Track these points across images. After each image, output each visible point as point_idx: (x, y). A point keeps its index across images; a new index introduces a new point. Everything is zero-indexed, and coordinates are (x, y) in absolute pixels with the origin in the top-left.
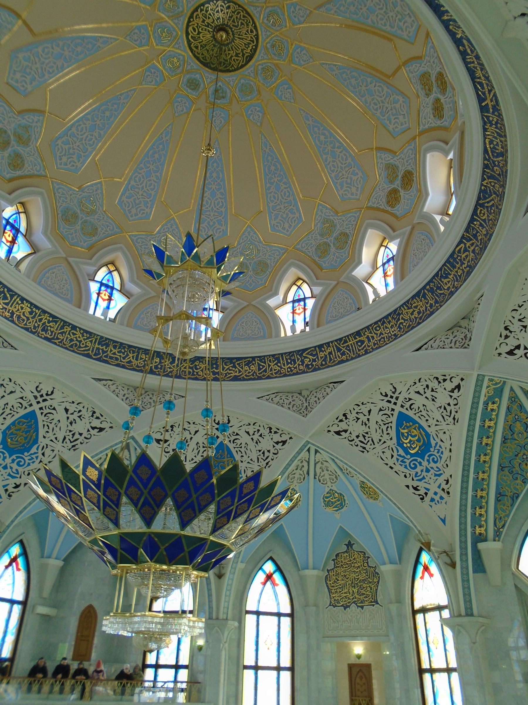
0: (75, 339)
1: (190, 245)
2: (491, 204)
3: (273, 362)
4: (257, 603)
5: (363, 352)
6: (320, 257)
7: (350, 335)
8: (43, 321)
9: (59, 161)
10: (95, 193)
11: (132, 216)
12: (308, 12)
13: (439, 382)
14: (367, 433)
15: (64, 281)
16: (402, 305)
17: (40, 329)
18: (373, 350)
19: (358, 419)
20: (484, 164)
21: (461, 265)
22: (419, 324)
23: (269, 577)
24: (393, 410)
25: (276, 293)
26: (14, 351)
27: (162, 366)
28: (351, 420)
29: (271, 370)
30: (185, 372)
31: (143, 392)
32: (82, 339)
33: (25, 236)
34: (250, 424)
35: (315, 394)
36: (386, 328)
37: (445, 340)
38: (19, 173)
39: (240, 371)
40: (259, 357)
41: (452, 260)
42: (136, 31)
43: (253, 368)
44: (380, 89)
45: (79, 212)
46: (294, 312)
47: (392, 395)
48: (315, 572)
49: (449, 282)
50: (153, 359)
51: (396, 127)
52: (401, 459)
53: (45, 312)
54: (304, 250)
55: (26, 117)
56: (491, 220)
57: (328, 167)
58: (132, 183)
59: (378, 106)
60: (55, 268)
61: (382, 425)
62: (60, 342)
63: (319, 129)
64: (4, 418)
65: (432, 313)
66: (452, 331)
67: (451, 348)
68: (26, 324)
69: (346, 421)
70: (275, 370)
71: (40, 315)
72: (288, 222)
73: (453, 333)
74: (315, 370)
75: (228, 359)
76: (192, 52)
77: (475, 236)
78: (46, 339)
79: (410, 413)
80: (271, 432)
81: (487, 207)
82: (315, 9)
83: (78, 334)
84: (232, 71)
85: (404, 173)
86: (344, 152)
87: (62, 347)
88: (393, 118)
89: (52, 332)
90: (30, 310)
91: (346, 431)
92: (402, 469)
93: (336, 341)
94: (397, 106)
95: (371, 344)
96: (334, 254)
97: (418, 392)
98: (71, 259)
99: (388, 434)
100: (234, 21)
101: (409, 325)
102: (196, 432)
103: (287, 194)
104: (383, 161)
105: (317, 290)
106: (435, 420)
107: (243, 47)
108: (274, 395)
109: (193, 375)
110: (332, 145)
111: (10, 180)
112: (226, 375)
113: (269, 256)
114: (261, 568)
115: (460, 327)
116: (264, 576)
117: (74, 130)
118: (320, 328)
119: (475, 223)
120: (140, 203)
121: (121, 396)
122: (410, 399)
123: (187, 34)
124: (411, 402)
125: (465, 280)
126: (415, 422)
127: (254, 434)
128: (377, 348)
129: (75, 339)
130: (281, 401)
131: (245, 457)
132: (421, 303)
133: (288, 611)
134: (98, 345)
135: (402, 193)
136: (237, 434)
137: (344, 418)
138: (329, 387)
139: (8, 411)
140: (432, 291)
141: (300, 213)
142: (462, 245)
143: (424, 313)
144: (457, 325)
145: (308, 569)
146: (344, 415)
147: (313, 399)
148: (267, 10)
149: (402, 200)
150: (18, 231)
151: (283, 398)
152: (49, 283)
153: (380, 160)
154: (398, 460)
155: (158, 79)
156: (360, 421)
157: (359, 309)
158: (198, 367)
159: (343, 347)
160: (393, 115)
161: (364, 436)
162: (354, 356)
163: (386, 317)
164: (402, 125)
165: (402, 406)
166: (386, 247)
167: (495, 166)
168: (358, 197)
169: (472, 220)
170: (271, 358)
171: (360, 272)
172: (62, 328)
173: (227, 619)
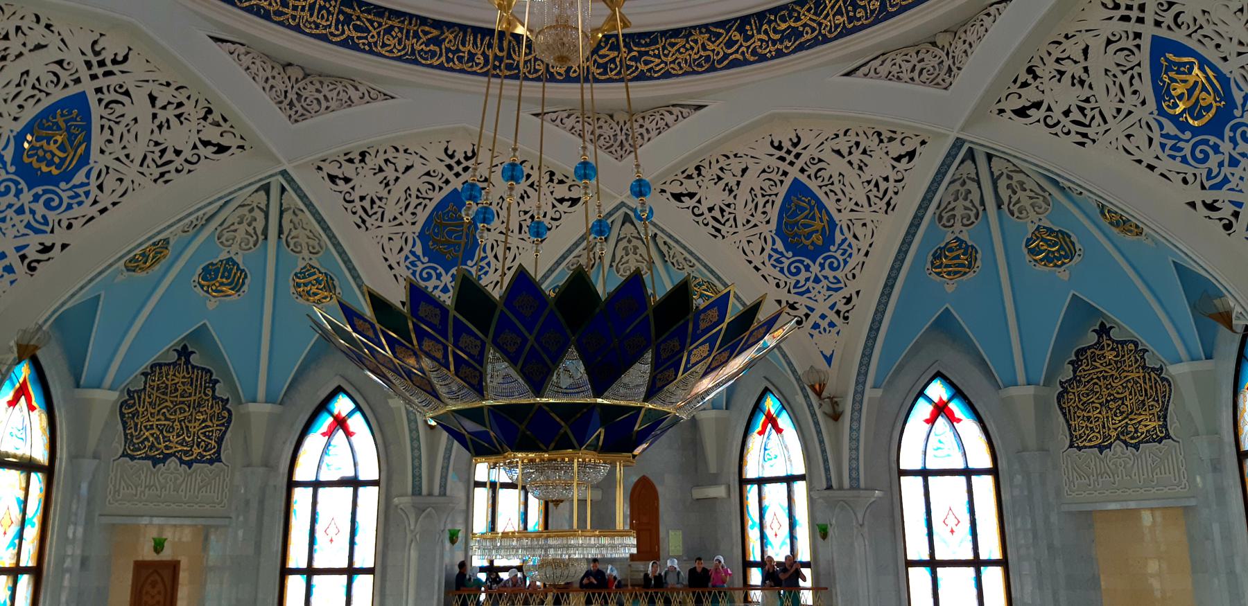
4: (921, 456)
23: (941, 409)
34: (837, 136)
48: (1031, 390)
52: (1170, 143)
64: (413, 214)
80: (881, 141)
92: (1177, 165)
102: (744, 171)
106: (1235, 41)
114: (921, 394)
116: (930, 408)
127: (850, 153)
131: (844, 202)
133: (987, 463)
136: (820, 160)
139: (414, 202)
145: (1016, 385)
154: (1163, 146)
173: (858, 488)
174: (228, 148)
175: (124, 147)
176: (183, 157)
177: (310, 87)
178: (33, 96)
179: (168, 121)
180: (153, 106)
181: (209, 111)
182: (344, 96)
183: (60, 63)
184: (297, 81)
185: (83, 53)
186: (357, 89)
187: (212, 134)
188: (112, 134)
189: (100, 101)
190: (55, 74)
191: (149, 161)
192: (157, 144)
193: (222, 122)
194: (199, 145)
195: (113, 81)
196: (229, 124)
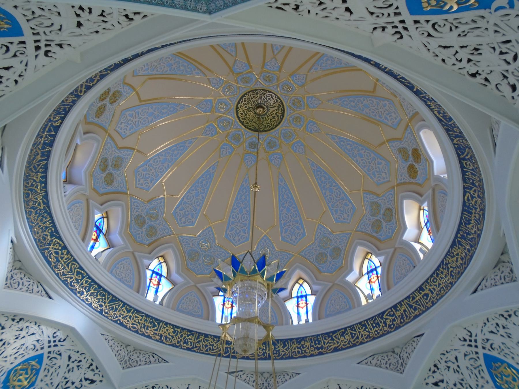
0: (209, 344)
1: (235, 263)
2: (469, 157)
3: (362, 328)
5: (430, 303)
6: (376, 232)
7: (415, 291)
8: (184, 336)
9: (180, 223)
10: (208, 235)
11: (236, 243)
12: (305, 76)
13: (506, 319)
14: (462, 380)
15: (195, 302)
16: (446, 256)
17: (182, 342)
18: (438, 300)
19: (449, 367)
20: (446, 129)
21: (476, 210)
22: (465, 268)
24: (477, 353)
25: (351, 270)
26: (167, 364)
27: (277, 351)
28: (443, 370)
29: (362, 336)
30: (295, 352)
31: (269, 375)
32: (213, 343)
33: (166, 278)
35: (405, 350)
36: (442, 278)
37: (496, 278)
38: (154, 238)
39: (338, 343)
40: (350, 327)
41: (466, 208)
42: (207, 129)
43: (347, 337)
44: (371, 102)
45: (199, 250)
46: (370, 281)
47: (470, 338)
49: (473, 226)
50: (269, 347)
51: (393, 122)
53: (183, 329)
54: (363, 230)
55: (153, 203)
56: (477, 168)
57: (360, 165)
58: (232, 220)
59: (375, 113)
60: (188, 295)
61: (473, 369)
62: (198, 349)
63: (344, 142)
65: (472, 257)
66: (497, 268)
67: (502, 283)
68: (172, 342)
69: (438, 372)
70: (365, 335)
71: (181, 332)
72: (346, 213)
73: (499, 269)
74: (397, 328)
75: (326, 334)
76: (245, 127)
77: (473, 184)
78: (188, 349)
79: (494, 353)
81: (468, 159)
82: (308, 72)
83: (211, 340)
84: (275, 128)
85: (412, 151)
86: (367, 151)
87: (200, 353)
88: (388, 116)
89: (191, 343)
90: (173, 330)
91: (442, 381)
93: (406, 299)
94: (387, 108)
95: (435, 295)
96: (386, 226)
97: (492, 332)
98: (198, 285)
99: (482, 377)
100: (264, 100)
101: (459, 272)
103: (339, 193)
104: (396, 148)
105: (382, 258)
107: (276, 111)
108: (371, 358)
109: (302, 353)
110: (357, 150)
111: (149, 245)
112: (328, 348)
113: (340, 242)
115: (504, 262)
117: (185, 200)
118: (390, 291)
119: (467, 174)
120: (240, 231)
121: (251, 383)
122: (488, 340)
123: (239, 118)
124: (490, 342)
125: (484, 222)
126: (503, 362)
128: (440, 298)
129: (209, 344)
130: (379, 362)
132: (459, 250)
134: (226, 344)
135: (417, 166)
137: (436, 370)
138: (414, 341)
140: (463, 237)
141: (352, 204)
142: (468, 194)
143: (465, 258)
144: (499, 262)
146: (435, 366)
147: (405, 355)
148: (280, 86)
149: (419, 172)
150: (161, 275)
151: (380, 358)
152: (184, 307)
153: (393, 148)
155: (230, 150)
156: (451, 369)
157: (414, 267)
158: (304, 346)
159: (414, 303)
160: (387, 115)
161: (461, 384)
162: (424, 309)
163: (438, 269)
164: (396, 119)
165: (484, 348)
166: (424, 210)
167: (453, 128)
168: (388, 179)
169: (464, 173)
170: (359, 326)
171: (409, 235)
172: (198, 338)
174: (95, 381)
175: (51, 379)
176: (74, 385)
177: (135, 355)
178: (22, 354)
179: (73, 368)
180: (69, 361)
181: (91, 365)
182: (148, 360)
183: (38, 341)
184: (131, 352)
185: (49, 337)
186: (154, 357)
187: (90, 375)
188: (48, 372)
189: (48, 357)
190: (35, 346)
191: (60, 386)
192: (65, 378)
193: (95, 369)
194: (83, 380)
195: (56, 349)
196: (98, 370)
